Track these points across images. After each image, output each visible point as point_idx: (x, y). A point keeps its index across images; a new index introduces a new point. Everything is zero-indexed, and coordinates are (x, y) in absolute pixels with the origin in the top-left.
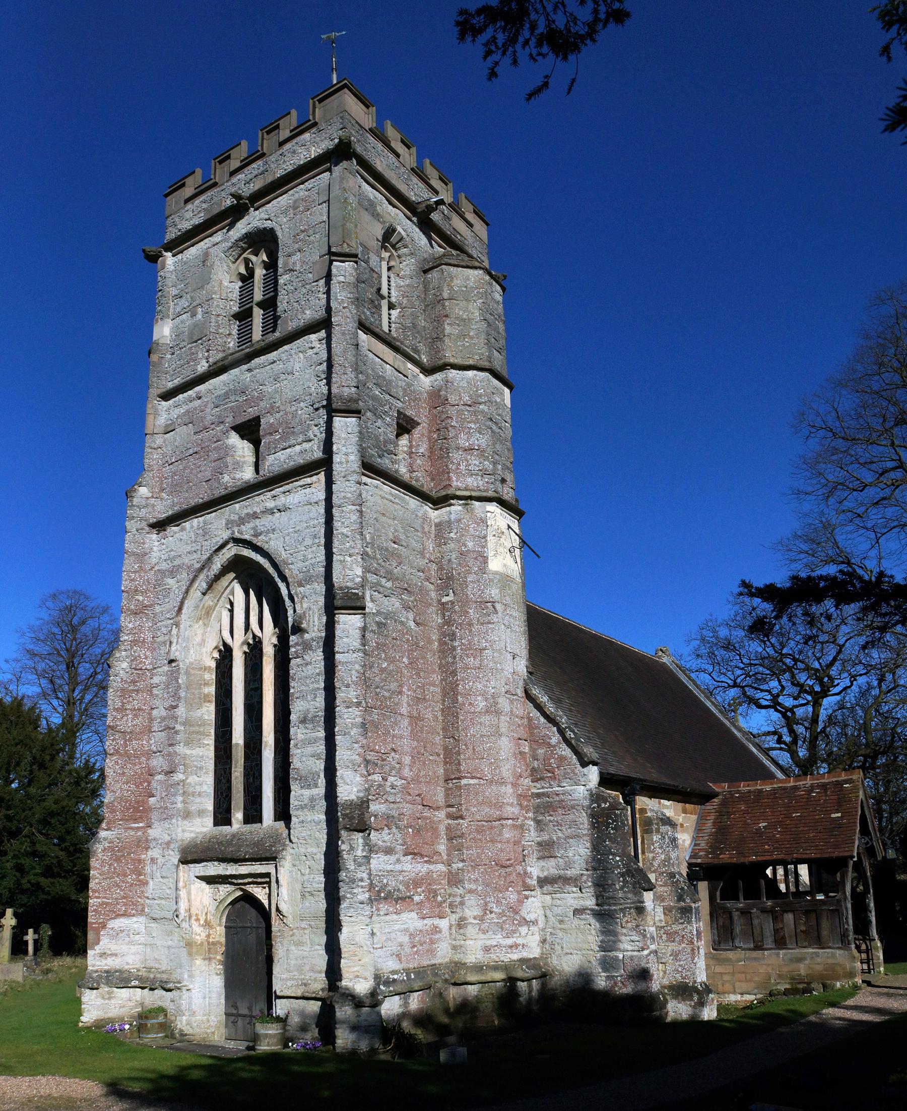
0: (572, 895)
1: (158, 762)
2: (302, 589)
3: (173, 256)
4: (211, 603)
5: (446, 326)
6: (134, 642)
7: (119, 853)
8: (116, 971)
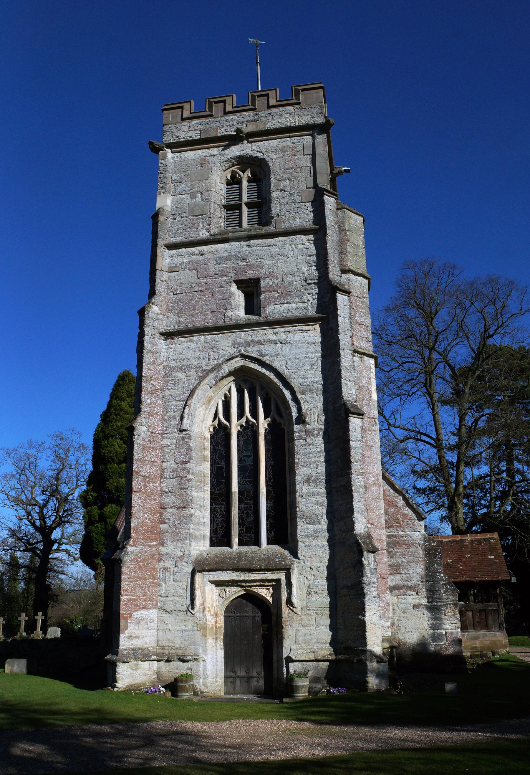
0: (412, 596)
1: (170, 500)
2: (303, 396)
3: (172, 152)
4: (213, 395)
5: (348, 247)
6: (151, 414)
7: (142, 563)
8: (139, 649)
